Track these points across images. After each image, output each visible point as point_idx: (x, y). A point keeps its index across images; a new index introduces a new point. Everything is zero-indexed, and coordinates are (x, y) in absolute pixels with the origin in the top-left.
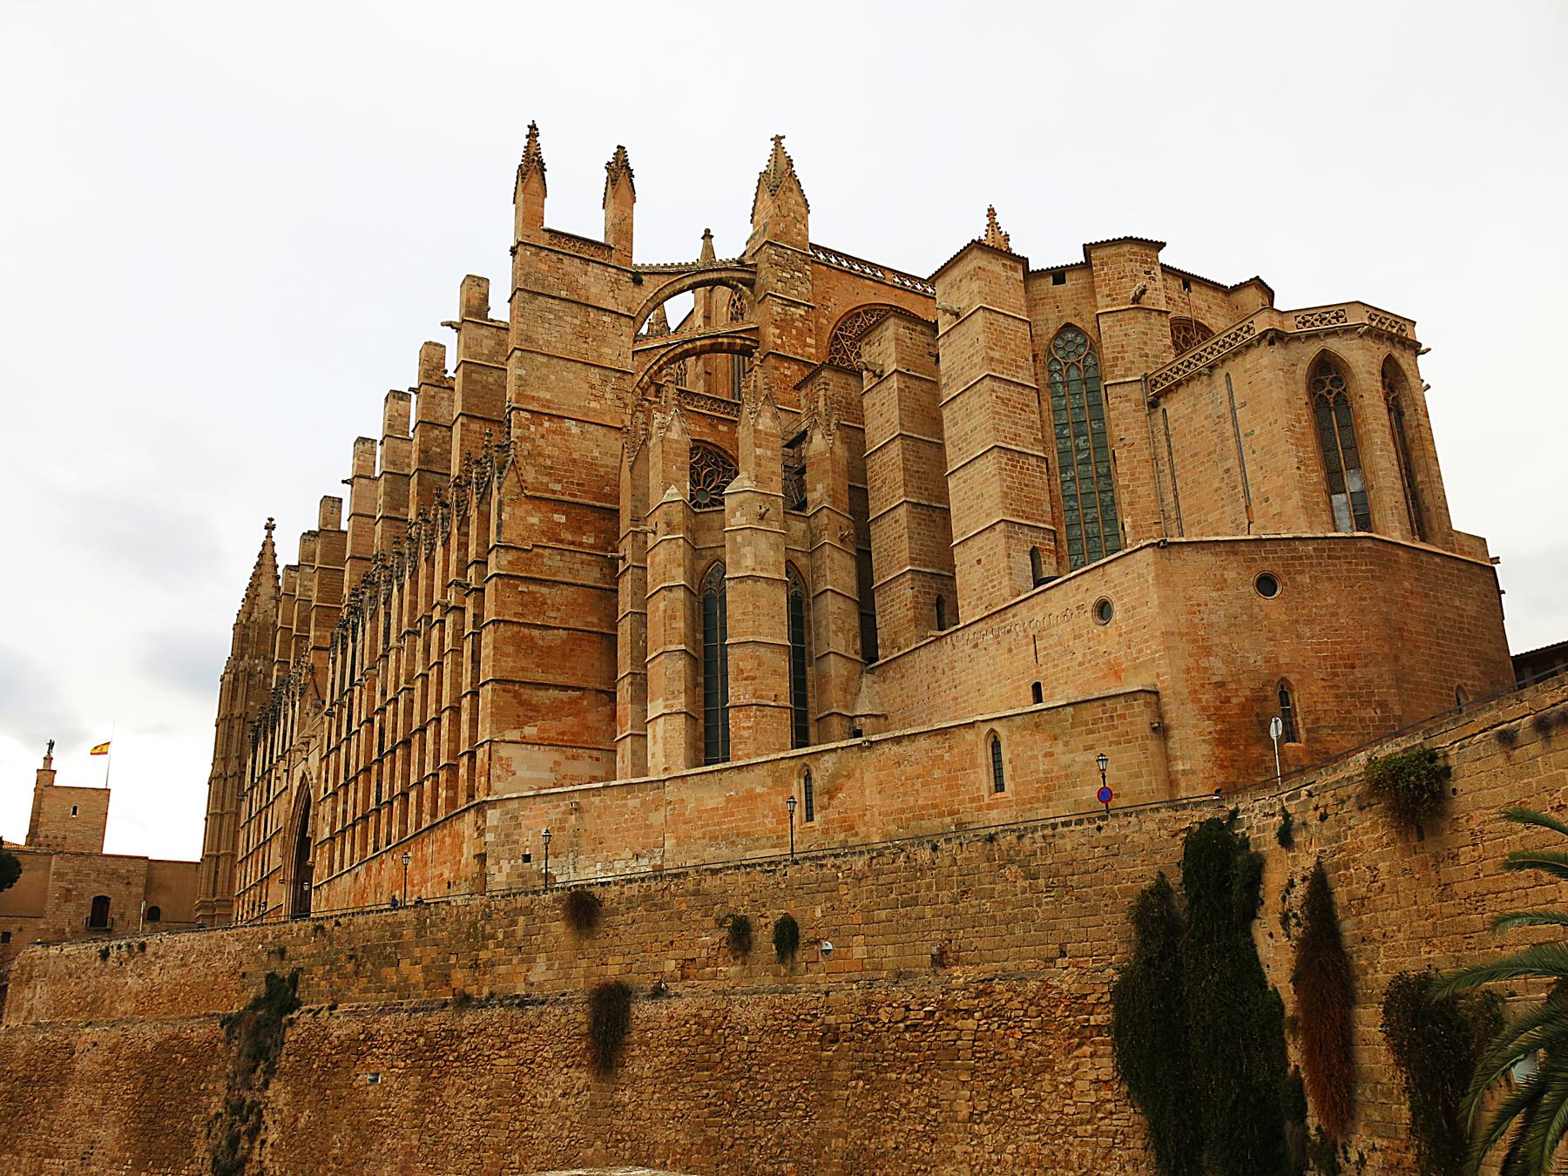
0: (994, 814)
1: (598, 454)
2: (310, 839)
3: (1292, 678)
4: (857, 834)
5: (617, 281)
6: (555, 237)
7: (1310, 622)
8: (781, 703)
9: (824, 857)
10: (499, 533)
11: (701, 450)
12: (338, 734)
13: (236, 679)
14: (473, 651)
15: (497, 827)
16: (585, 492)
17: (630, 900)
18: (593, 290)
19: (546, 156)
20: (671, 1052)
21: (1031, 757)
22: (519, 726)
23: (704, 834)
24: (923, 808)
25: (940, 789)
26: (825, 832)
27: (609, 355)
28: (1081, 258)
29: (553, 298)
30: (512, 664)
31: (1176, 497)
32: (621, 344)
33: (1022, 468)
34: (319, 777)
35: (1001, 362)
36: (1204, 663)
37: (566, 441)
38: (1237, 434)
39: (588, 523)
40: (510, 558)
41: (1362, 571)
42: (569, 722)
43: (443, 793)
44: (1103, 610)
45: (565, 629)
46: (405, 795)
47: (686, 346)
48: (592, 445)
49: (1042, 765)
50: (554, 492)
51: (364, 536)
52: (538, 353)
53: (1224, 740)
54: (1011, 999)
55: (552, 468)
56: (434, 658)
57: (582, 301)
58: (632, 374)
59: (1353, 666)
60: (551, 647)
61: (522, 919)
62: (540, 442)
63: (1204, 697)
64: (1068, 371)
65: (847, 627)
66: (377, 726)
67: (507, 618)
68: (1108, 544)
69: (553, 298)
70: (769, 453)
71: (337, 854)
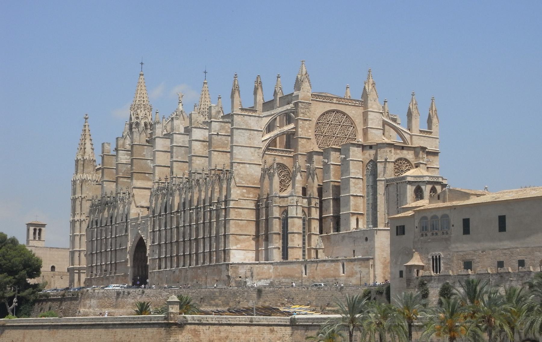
0: (342, 278)
4: (315, 279)
5: (258, 120)
17: (270, 291)
18: (252, 124)
22: (236, 245)
26: (309, 278)
27: (256, 143)
36: (382, 253)
39: (251, 191)
45: (246, 220)
50: (243, 184)
55: (242, 177)
60: (243, 225)
61: (246, 293)
62: (240, 170)
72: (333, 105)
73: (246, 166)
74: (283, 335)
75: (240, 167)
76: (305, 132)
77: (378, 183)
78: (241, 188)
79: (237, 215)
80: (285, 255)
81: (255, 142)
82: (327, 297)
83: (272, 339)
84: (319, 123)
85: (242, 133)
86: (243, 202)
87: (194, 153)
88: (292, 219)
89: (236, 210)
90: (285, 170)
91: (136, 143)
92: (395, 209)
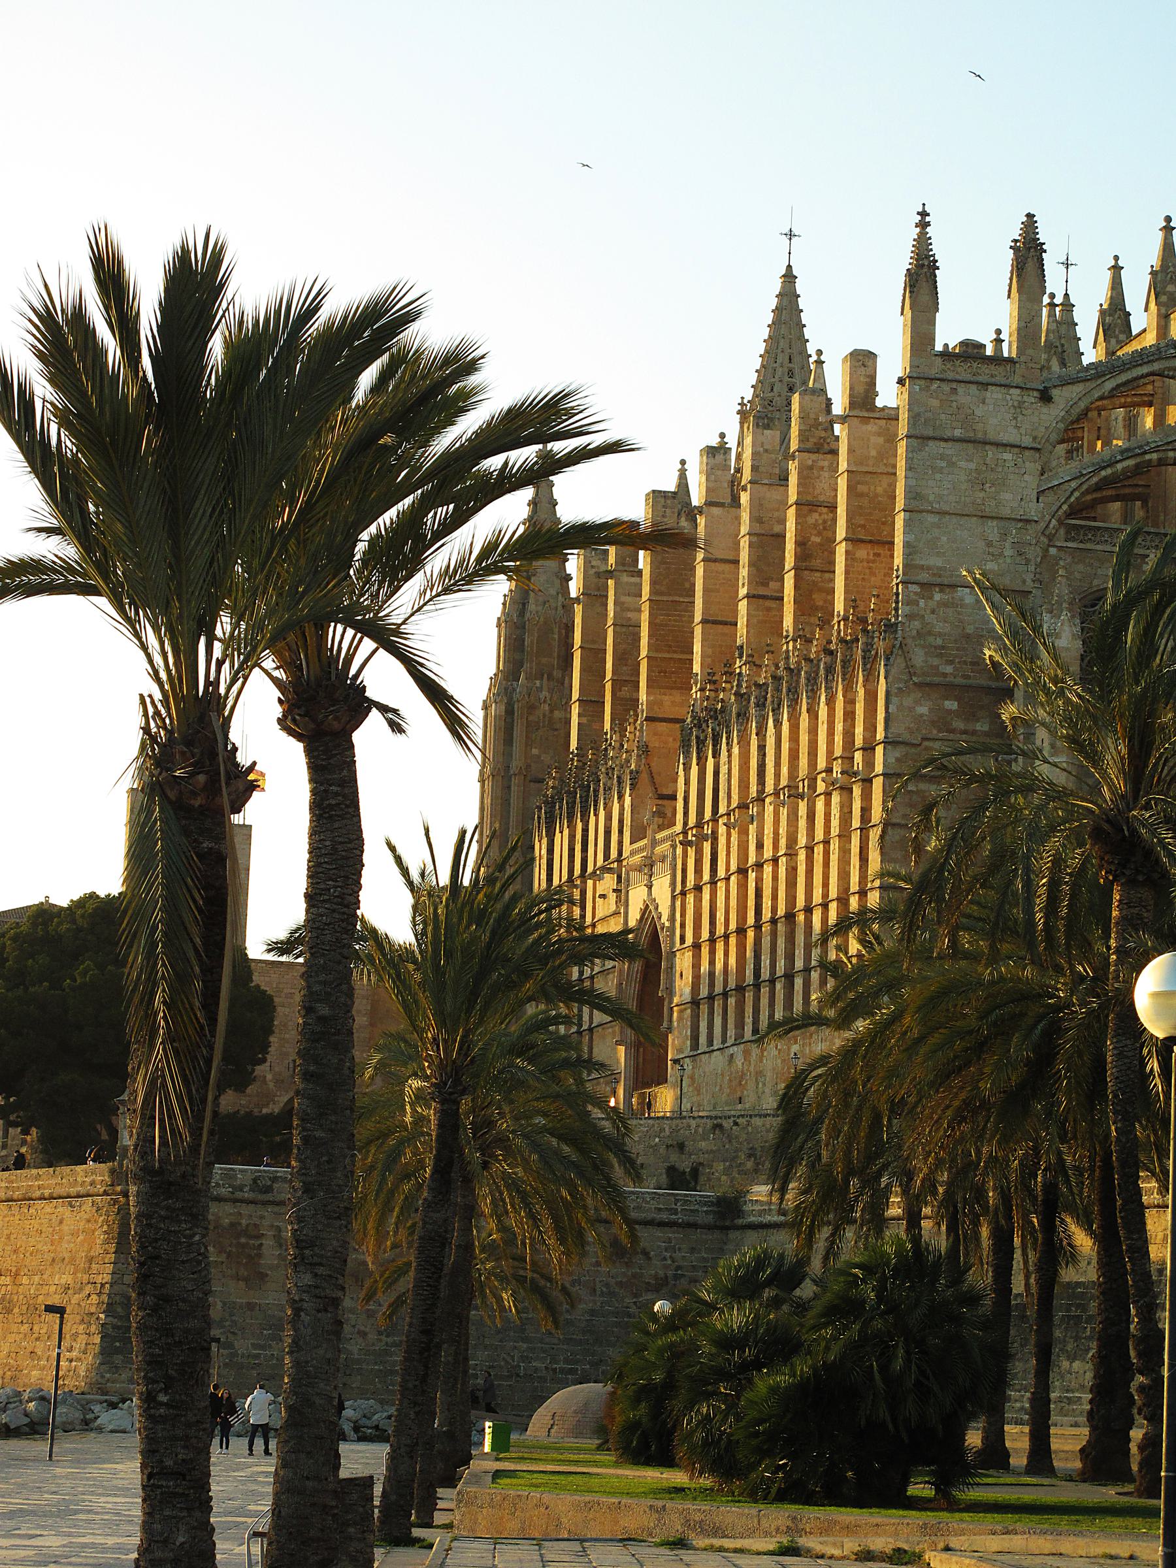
2: (662, 999)
5: (1021, 405)
10: (886, 728)
13: (509, 712)
14: (861, 847)
18: (993, 421)
19: (939, 249)
34: (672, 918)
40: (898, 755)
47: (1103, 473)
50: (945, 675)
51: (718, 591)
52: (928, 511)
55: (943, 648)
57: (980, 435)
58: (1036, 521)
67: (894, 821)
69: (946, 440)
71: (703, 1025)
74: (678, 1268)
75: (932, 604)
81: (1006, 496)
83: (620, 1284)
85: (942, 457)
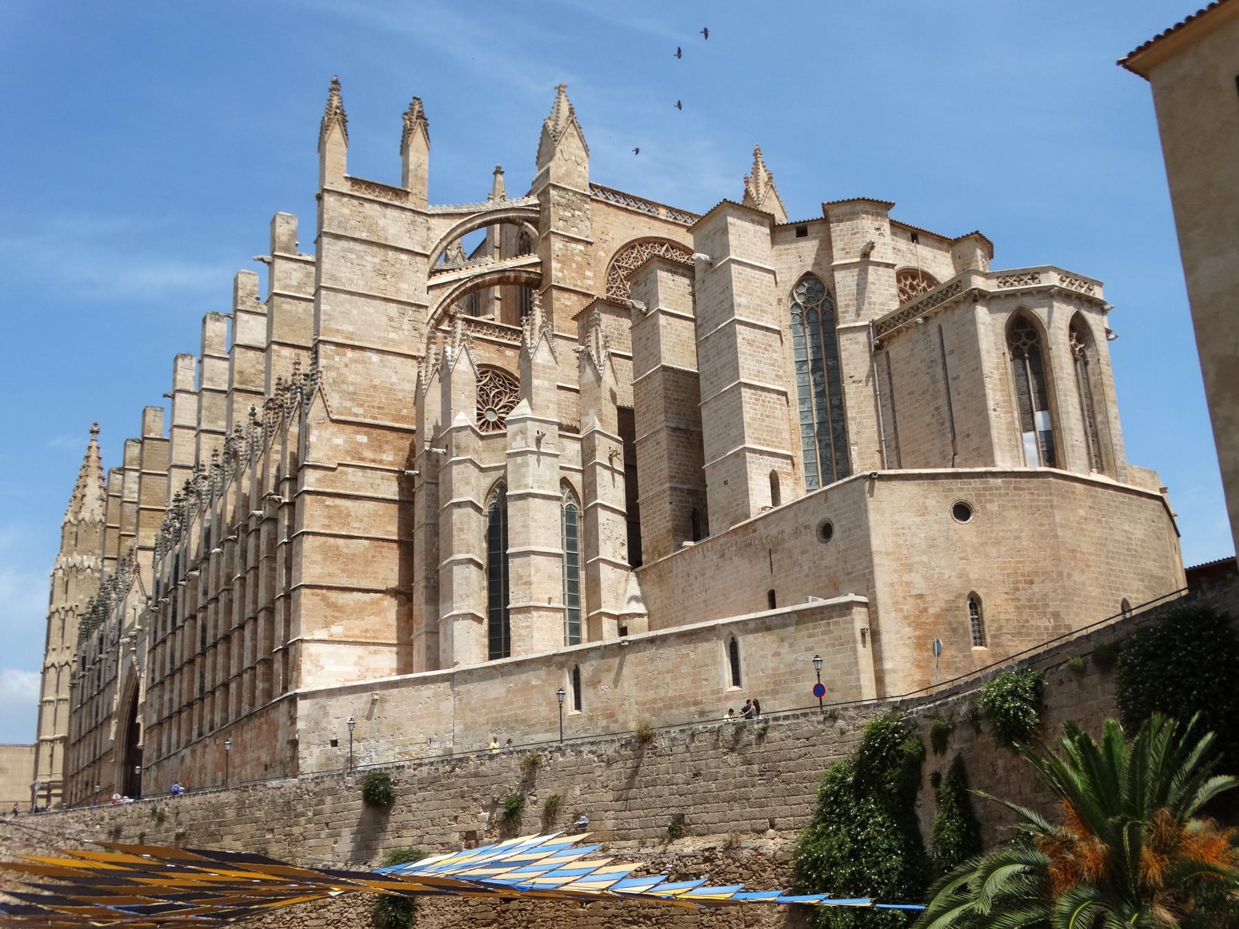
1: (396, 381)
3: (981, 593)
4: (616, 721)
5: (413, 223)
6: (357, 184)
7: (997, 543)
8: (553, 605)
9: (582, 744)
11: (490, 374)
12: (164, 629)
15: (308, 716)
16: (385, 414)
17: (420, 781)
20: (455, 912)
21: (762, 657)
22: (327, 625)
23: (488, 720)
24: (671, 698)
25: (686, 683)
26: (591, 718)
28: (820, 214)
29: (355, 240)
30: (320, 570)
31: (895, 428)
32: (416, 279)
33: (764, 401)
35: (748, 307)
36: (906, 578)
37: (367, 369)
38: (946, 378)
39: (387, 442)
41: (1042, 501)
42: (371, 621)
43: (260, 685)
44: (826, 531)
45: (367, 538)
46: (226, 685)
48: (391, 372)
49: (771, 663)
50: (356, 415)
53: (920, 644)
54: (729, 865)
55: (355, 394)
56: (251, 562)
59: (1031, 582)
60: (354, 555)
61: (329, 799)
62: (345, 371)
63: (905, 607)
64: (807, 314)
65: (615, 535)
66: (199, 623)
68: (839, 466)
69: (355, 240)
70: (546, 384)
72: (657, 224)
73: (369, 358)
75: (345, 360)
76: (573, 275)
77: (844, 342)
78: (348, 428)
79: (330, 517)
80: (499, 641)
81: (403, 286)
82: (669, 783)
84: (620, 268)
85: (351, 251)
86: (354, 476)
87: (241, 383)
88: (520, 503)
89: (329, 501)
90: (511, 390)
91: (152, 435)
92: (928, 418)
